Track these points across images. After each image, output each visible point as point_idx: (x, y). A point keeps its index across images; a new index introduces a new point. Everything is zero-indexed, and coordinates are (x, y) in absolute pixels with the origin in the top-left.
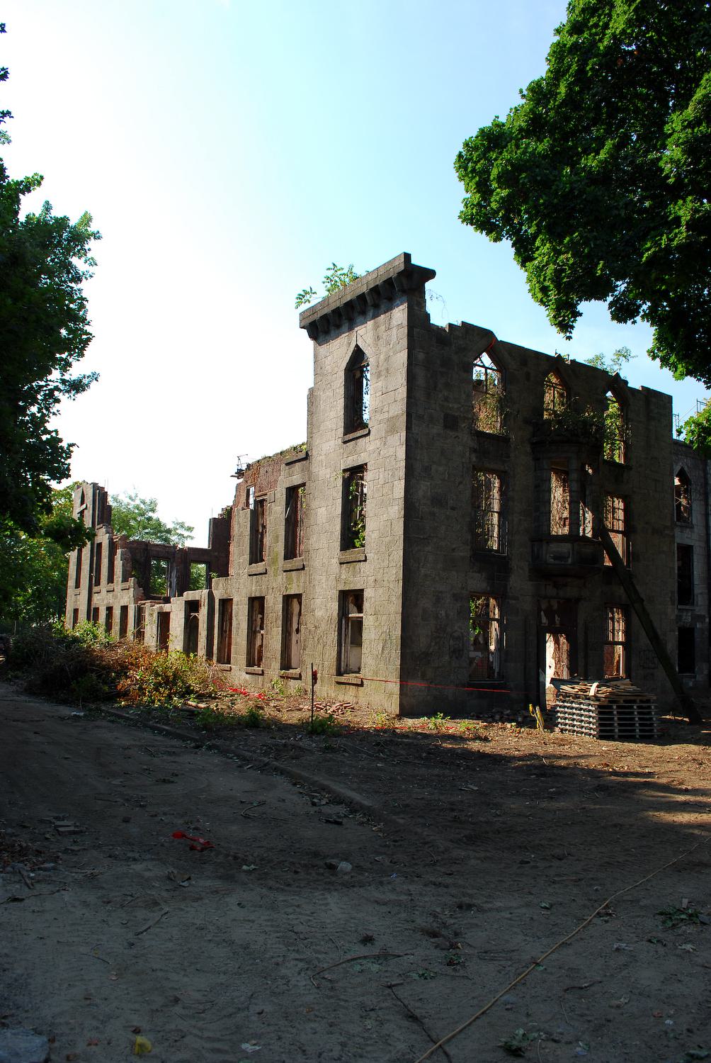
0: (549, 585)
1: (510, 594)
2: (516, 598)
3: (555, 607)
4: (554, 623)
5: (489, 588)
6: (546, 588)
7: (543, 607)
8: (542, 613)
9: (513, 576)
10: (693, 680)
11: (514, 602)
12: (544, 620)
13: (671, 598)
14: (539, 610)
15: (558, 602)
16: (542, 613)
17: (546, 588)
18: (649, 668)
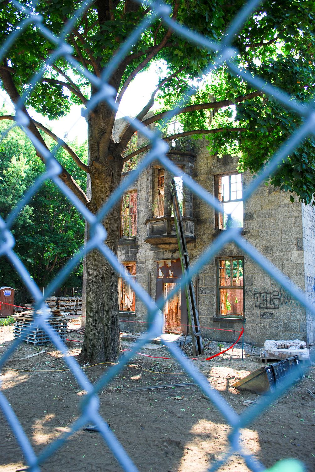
0: (166, 251)
1: (139, 261)
2: (143, 263)
3: (169, 264)
4: (169, 276)
5: (126, 259)
6: (163, 253)
7: (161, 266)
8: (160, 270)
9: (140, 249)
11: (141, 265)
12: (161, 274)
13: (296, 244)
14: (158, 268)
15: (172, 262)
16: (160, 270)
17: (163, 253)
18: (267, 308)
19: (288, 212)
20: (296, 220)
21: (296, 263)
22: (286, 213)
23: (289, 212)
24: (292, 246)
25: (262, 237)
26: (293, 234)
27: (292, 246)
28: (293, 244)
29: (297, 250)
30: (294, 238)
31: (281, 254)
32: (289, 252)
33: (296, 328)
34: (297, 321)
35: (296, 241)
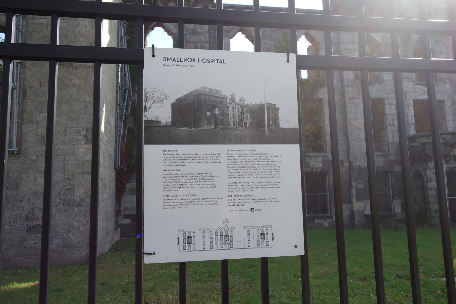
10: (330, 220)
19: (77, 94)
20: (87, 106)
21: (83, 159)
22: (74, 96)
23: (78, 95)
24: (80, 138)
25: (37, 123)
26: (82, 123)
27: (80, 138)
28: (81, 135)
29: (86, 143)
30: (83, 128)
31: (64, 147)
32: (74, 145)
33: (78, 242)
34: (80, 233)
35: (85, 132)
